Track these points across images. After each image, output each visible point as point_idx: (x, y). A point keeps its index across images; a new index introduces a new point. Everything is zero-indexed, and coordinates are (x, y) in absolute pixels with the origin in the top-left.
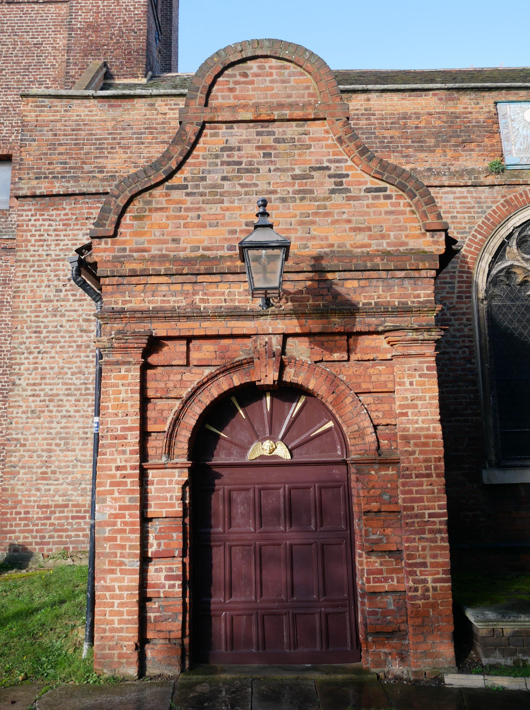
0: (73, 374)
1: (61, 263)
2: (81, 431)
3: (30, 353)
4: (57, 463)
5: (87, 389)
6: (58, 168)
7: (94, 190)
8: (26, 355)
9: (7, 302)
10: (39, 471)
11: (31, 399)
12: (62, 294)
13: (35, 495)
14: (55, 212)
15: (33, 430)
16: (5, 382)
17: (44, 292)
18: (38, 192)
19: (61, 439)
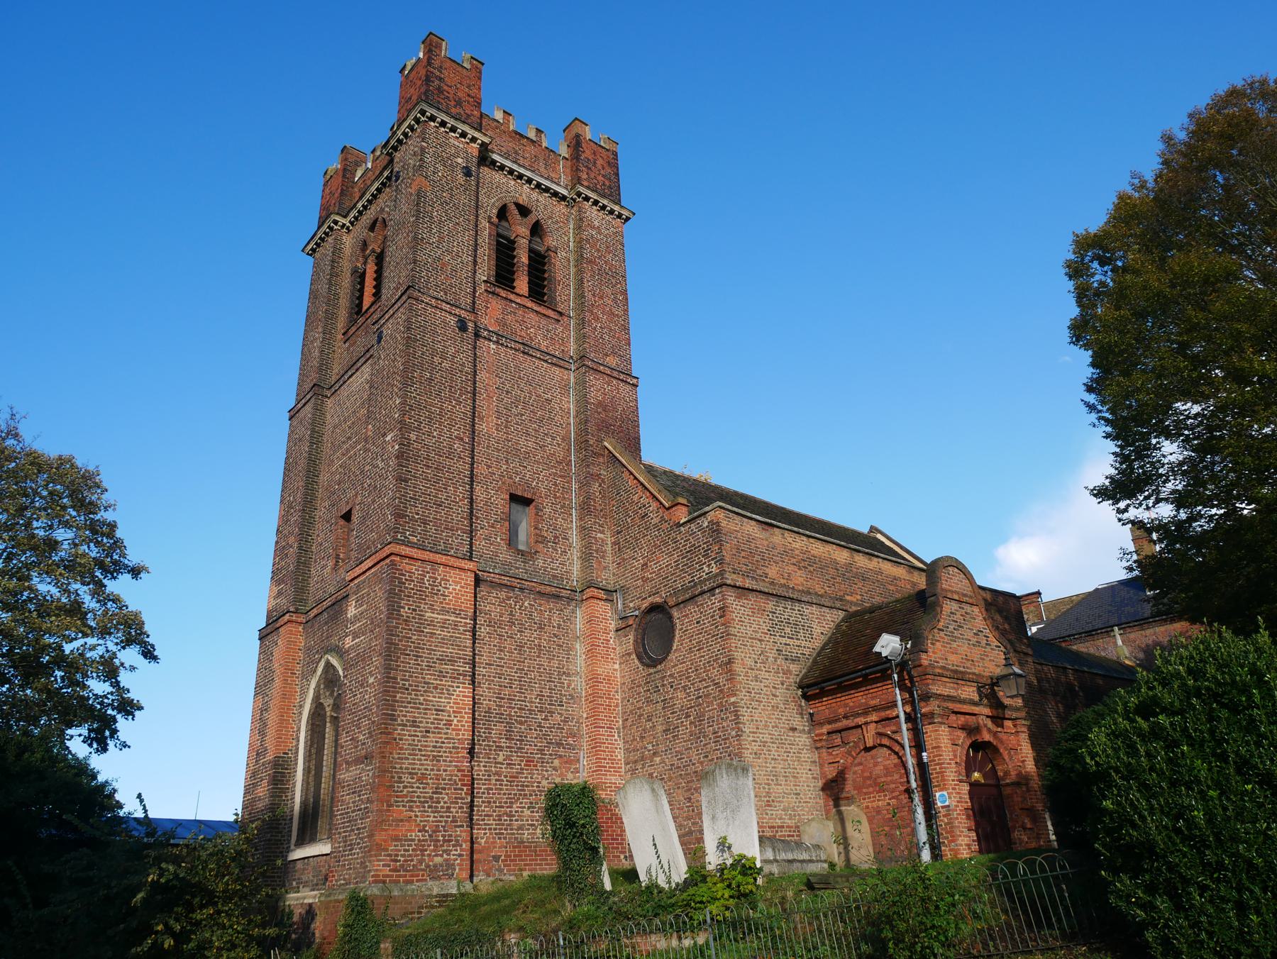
2: (782, 770)
3: (748, 708)
5: (781, 739)
7: (766, 590)
8: (745, 709)
9: (544, 647)
11: (753, 743)
12: (758, 665)
13: (765, 818)
15: (758, 768)
17: (750, 662)
18: (738, 584)
19: (774, 776)
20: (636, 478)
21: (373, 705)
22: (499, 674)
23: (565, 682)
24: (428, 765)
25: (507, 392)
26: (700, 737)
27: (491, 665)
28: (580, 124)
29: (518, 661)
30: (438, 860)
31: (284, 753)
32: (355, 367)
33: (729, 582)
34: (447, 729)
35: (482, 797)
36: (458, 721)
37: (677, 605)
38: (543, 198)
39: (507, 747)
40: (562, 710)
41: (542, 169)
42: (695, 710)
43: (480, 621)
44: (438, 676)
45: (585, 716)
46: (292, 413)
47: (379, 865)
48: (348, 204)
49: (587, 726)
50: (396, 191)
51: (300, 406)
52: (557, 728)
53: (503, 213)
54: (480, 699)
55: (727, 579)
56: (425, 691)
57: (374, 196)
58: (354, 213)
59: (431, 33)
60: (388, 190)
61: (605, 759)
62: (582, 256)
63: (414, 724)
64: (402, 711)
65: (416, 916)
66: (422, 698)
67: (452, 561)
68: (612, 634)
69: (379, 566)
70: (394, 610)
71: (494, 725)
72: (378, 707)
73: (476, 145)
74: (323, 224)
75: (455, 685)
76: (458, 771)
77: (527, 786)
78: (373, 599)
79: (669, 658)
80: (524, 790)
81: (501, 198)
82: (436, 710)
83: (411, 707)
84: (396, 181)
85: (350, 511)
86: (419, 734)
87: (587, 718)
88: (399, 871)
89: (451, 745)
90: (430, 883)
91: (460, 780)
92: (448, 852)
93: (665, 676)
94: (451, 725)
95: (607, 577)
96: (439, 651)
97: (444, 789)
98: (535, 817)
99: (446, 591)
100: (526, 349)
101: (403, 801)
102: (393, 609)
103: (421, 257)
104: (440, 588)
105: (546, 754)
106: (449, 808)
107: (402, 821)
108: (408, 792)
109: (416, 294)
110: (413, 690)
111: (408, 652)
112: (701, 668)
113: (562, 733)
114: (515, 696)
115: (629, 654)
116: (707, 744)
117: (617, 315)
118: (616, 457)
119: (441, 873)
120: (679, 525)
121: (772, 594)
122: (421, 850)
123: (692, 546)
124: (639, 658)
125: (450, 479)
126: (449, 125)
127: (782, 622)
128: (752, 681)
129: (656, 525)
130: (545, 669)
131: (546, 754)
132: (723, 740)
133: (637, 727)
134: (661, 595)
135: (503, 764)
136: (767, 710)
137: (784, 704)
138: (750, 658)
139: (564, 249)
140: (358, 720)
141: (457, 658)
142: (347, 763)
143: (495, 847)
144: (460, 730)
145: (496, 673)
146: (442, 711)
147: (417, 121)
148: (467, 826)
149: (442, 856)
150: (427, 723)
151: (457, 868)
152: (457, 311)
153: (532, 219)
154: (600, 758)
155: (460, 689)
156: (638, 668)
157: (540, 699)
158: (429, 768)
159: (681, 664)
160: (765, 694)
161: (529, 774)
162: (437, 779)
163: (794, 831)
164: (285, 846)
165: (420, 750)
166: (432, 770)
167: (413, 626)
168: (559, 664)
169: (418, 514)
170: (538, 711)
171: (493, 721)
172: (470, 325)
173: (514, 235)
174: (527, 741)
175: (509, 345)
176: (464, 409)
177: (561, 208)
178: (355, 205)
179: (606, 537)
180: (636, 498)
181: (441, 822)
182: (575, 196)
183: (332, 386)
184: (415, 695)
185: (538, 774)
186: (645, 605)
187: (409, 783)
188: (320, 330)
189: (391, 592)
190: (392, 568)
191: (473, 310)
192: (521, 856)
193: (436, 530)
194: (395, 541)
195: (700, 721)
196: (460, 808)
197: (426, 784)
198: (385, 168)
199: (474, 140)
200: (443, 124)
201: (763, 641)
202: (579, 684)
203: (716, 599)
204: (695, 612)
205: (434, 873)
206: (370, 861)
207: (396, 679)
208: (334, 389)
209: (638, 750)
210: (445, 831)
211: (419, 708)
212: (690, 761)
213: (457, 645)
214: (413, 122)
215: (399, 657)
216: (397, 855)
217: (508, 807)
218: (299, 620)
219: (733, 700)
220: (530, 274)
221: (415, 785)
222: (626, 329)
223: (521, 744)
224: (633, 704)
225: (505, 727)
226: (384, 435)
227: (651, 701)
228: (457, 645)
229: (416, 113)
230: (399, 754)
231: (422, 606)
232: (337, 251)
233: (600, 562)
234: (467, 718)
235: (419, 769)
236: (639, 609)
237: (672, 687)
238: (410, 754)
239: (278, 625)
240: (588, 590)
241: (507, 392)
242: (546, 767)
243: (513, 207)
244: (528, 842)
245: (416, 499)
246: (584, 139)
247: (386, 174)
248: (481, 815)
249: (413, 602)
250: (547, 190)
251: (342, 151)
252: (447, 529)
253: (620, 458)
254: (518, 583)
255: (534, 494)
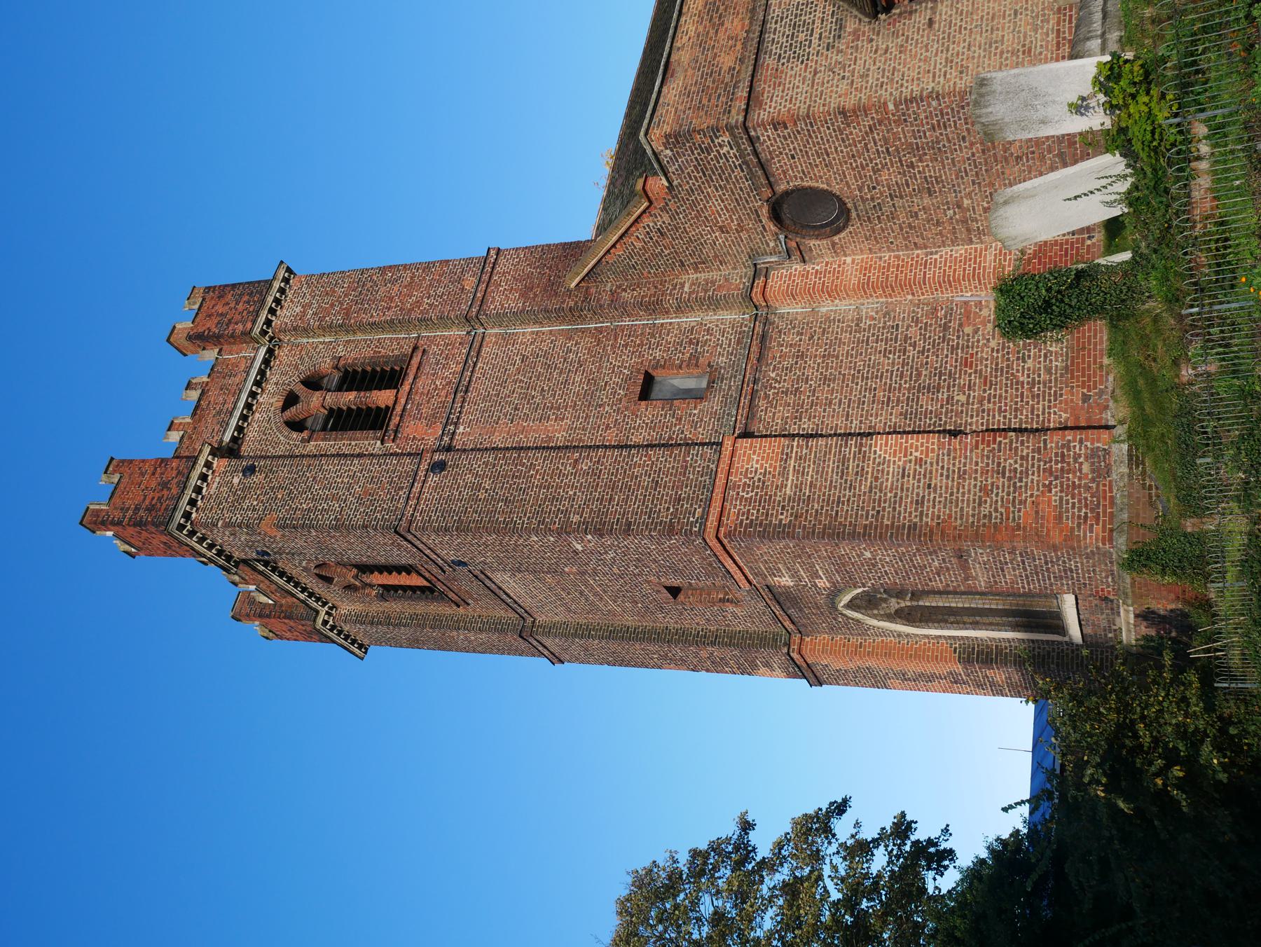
0: (927, 51)
1: (816, 81)
2: (984, 35)
3: (902, 86)
4: (1015, 45)
5: (943, 38)
6: (723, 99)
7: (751, 68)
8: (904, 89)
9: (825, 350)
10: (1021, 56)
11: (948, 76)
12: (847, 74)
13: (1046, 55)
14: (765, 95)
16: (924, 342)
17: (844, 86)
18: (743, 107)
19: (990, 46)
20: (614, 246)
21: (897, 551)
22: (859, 404)
23: (868, 323)
24: (970, 484)
25: (516, 409)
26: (939, 148)
27: (848, 415)
28: (174, 336)
29: (843, 382)
30: (1086, 468)
31: (955, 652)
32: (497, 591)
33: (741, 119)
34: (926, 463)
35: (1010, 419)
36: (917, 451)
37: (771, 185)
38: (273, 377)
39: (948, 391)
40: (903, 327)
41: (237, 380)
42: (905, 155)
43: (794, 430)
44: (862, 476)
45: (910, 297)
46: (555, 660)
47: (1091, 537)
48: (302, 610)
49: (923, 294)
50: (281, 554)
51: (546, 652)
52: (926, 330)
53: (296, 425)
54: (890, 426)
55: (737, 122)
56: (881, 491)
57: (290, 579)
58: (312, 602)
59: (81, 523)
60: (280, 564)
61: (964, 269)
62: (341, 326)
63: (920, 503)
64: (905, 517)
65: (1154, 491)
66: (889, 495)
67: (724, 466)
68: (809, 267)
69: (732, 552)
70: (784, 531)
71: (922, 407)
72: (899, 546)
73: (215, 462)
74: (329, 638)
75: (872, 456)
76: (977, 448)
77: (997, 364)
78: (772, 556)
79: (838, 193)
80: (1002, 368)
81: (278, 428)
82: (903, 477)
83: (900, 507)
84: (268, 554)
85: (667, 588)
86: (932, 496)
87: (913, 294)
88: (1098, 513)
89: (946, 458)
90: (1114, 476)
91: (988, 446)
92: (1078, 456)
93: (861, 197)
94: (921, 459)
95: (738, 276)
96: (832, 477)
97: (999, 464)
98: (1035, 353)
99: (759, 471)
100: (461, 389)
101: (1013, 512)
102: (783, 532)
103: (359, 520)
104: (756, 479)
105: (958, 343)
106: (1022, 458)
107: (1037, 512)
108: (1002, 507)
109: (404, 523)
110: (879, 506)
111: (834, 513)
112: (851, 150)
113: (931, 325)
114: (886, 383)
115: (834, 244)
116: (948, 138)
117: (411, 278)
118: (589, 272)
119: (1103, 464)
120: (671, 187)
121: (756, 60)
122: (1074, 489)
123: (697, 169)
124: (838, 231)
125: (625, 472)
126: (194, 495)
127: (791, 45)
128: (867, 82)
129: (672, 218)
130: (853, 349)
131: (958, 343)
132: (942, 117)
133: (925, 230)
134: (760, 207)
135: (969, 395)
136: (905, 59)
137: (897, 37)
138: (837, 86)
139: (334, 348)
140: (915, 568)
141: (840, 455)
142: (967, 579)
143: (1072, 400)
144: (927, 447)
145: (858, 407)
146: (904, 470)
147: (192, 533)
148: (1045, 435)
149: (1081, 464)
150: (919, 487)
151: (1097, 445)
152: (421, 474)
153: (300, 390)
154: (964, 276)
155: (878, 449)
156: (851, 233)
157: (890, 353)
158: (973, 483)
159: (845, 177)
160: (885, 63)
161: (981, 362)
162: (987, 473)
163: (1065, 15)
164: (1065, 647)
165: (952, 494)
166: (976, 479)
167: (802, 508)
168: (846, 332)
169: (668, 509)
170: (904, 355)
171: (917, 409)
172: (437, 457)
173: (322, 410)
174: (941, 367)
175: (459, 410)
176: (538, 458)
177: (283, 354)
178: (303, 602)
179: (689, 280)
180: (639, 245)
181: (1039, 466)
182: (267, 338)
183: (521, 616)
184: (885, 502)
185: (982, 352)
186: (772, 227)
187: (991, 506)
188: (455, 633)
189: (762, 536)
190: (734, 535)
191: (419, 455)
192: (1084, 368)
193: (686, 487)
194: (701, 533)
195: (918, 148)
196: (1022, 443)
197: (992, 485)
198: (255, 569)
199: (208, 465)
200: (192, 502)
201: (816, 69)
202: (871, 306)
203: (763, 135)
204: (779, 161)
205: (1102, 472)
206: (1086, 548)
207: (866, 526)
208: (523, 614)
209: (954, 228)
210: (1051, 461)
211: (901, 498)
212: (969, 159)
213: (825, 456)
214: (194, 539)
215: (840, 523)
216: (1079, 517)
217: (1023, 387)
218: (798, 641)
219: (891, 107)
220: (369, 389)
221: (994, 499)
222: (428, 266)
223: (945, 374)
224: (895, 237)
225: (923, 394)
226: (576, 552)
227: (892, 214)
228: (825, 456)
229: (183, 536)
230: (956, 518)
231: (778, 498)
232: (359, 619)
233: (720, 286)
234: (912, 440)
235: (975, 495)
236: (777, 234)
237: (874, 188)
238: (957, 506)
239: (805, 665)
240: (755, 300)
241: (516, 409)
242: (973, 343)
243: (288, 413)
244: (1067, 360)
245: (651, 512)
246: (192, 329)
247: (261, 568)
248: (1032, 419)
249: (773, 509)
250: (262, 373)
251: (238, 620)
252: (685, 473)
253: (590, 266)
254: (748, 386)
255: (638, 371)
